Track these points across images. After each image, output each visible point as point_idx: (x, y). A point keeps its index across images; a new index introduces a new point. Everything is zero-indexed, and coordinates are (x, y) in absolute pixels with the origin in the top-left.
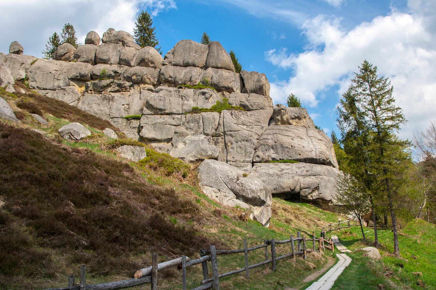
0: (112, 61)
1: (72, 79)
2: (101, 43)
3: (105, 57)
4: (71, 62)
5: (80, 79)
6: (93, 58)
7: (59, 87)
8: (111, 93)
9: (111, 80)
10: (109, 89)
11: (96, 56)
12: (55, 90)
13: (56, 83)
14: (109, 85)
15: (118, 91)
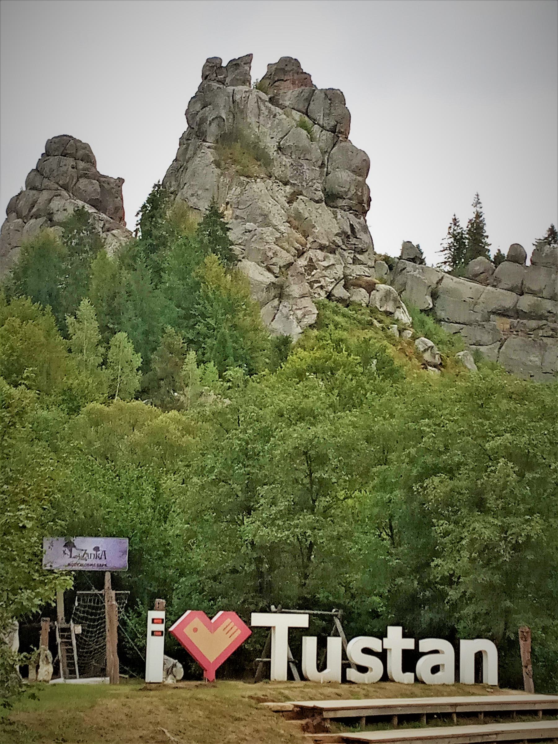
0: (545, 294)
1: (494, 313)
2: (528, 263)
3: (535, 288)
4: (489, 288)
5: (503, 313)
6: (520, 285)
7: (477, 322)
8: (543, 338)
9: (544, 322)
10: (541, 333)
11: (522, 284)
12: (471, 325)
13: (473, 318)
14: (540, 328)
15: (552, 336)
